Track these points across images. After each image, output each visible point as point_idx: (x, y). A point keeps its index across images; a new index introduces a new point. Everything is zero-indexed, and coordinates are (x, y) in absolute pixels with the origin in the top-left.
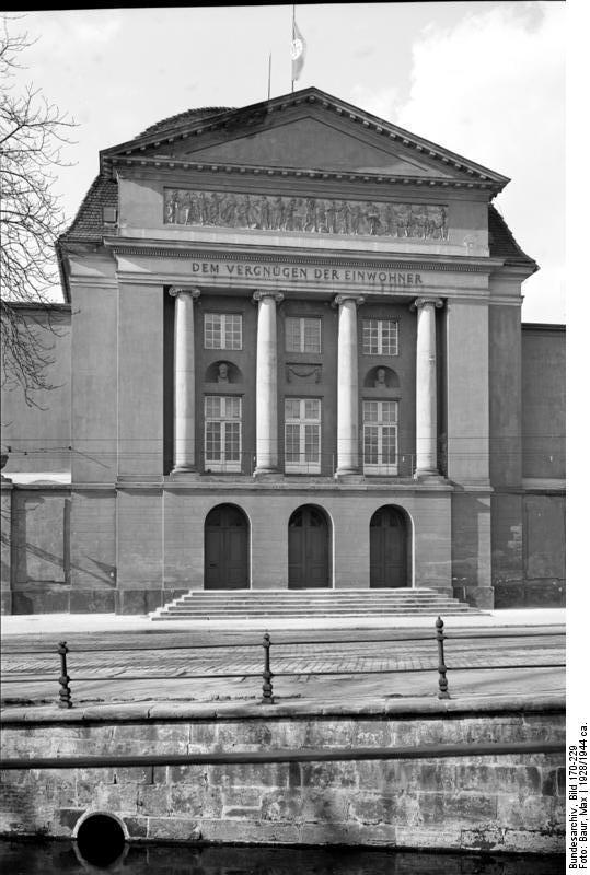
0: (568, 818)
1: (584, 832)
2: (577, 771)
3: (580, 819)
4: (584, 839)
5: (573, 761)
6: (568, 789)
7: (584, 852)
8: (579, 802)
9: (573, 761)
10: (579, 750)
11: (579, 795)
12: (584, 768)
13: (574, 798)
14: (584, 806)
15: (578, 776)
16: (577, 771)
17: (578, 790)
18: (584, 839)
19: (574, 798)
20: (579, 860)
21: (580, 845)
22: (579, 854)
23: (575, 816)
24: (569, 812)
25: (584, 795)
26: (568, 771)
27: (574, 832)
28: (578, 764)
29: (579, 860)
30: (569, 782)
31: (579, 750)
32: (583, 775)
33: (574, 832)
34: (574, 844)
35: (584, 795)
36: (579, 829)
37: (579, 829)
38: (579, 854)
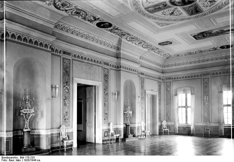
0: (15, 156)
1: (11, 160)
2: (28, 159)
3: (15, 159)
4: (10, 160)
5: (31, 157)
6: (23, 156)
7: (6, 161)
8: (20, 159)
9: (31, 157)
10: (33, 159)
11: (21, 159)
12: (29, 160)
13: (21, 158)
14: (18, 160)
15: (26, 159)
16: (28, 159)
17: (23, 159)
18: (10, 160)
19: (21, 158)
20: (4, 159)
22: (6, 159)
23: (16, 158)
24: (17, 156)
25: (21, 160)
26: (28, 156)
27: (11, 158)
28: (30, 159)
29: (4, 159)
30: (25, 156)
31: (33, 159)
33: (11, 158)
34: (8, 158)
35: (21, 160)
36: (12, 159)
37: (12, 159)
38: (6, 159)
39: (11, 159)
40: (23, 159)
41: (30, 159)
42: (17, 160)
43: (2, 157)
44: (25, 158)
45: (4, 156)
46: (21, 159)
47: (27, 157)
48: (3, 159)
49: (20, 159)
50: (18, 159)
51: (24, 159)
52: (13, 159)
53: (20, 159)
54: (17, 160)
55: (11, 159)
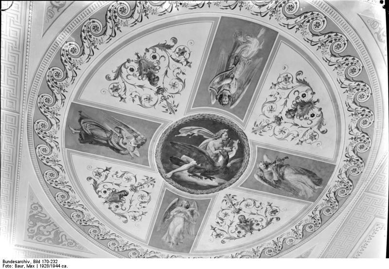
1: (19, 267)
2: (46, 263)
3: (25, 265)
4: (16, 266)
5: (51, 261)
7: (10, 267)
8: (32, 264)
9: (51, 261)
10: (56, 264)
11: (35, 264)
12: (48, 266)
13: (34, 262)
14: (31, 266)
15: (44, 264)
16: (46, 263)
17: (38, 264)
18: (16, 266)
19: (34, 262)
20: (7, 264)
22: (9, 264)
23: (26, 262)
25: (36, 266)
28: (49, 264)
29: (7, 264)
30: (41, 260)
31: (56, 264)
33: (19, 262)
35: (36, 266)
36: (21, 264)
37: (21, 264)
38: (9, 264)
39: (18, 264)
40: (39, 264)
41: (49, 264)
42: (28, 265)
44: (41, 263)
46: (35, 264)
47: (44, 261)
48: (5, 263)
49: (34, 264)
50: (30, 263)
51: (40, 264)
52: (22, 264)
53: (34, 264)
54: (28, 265)
55: (18, 264)
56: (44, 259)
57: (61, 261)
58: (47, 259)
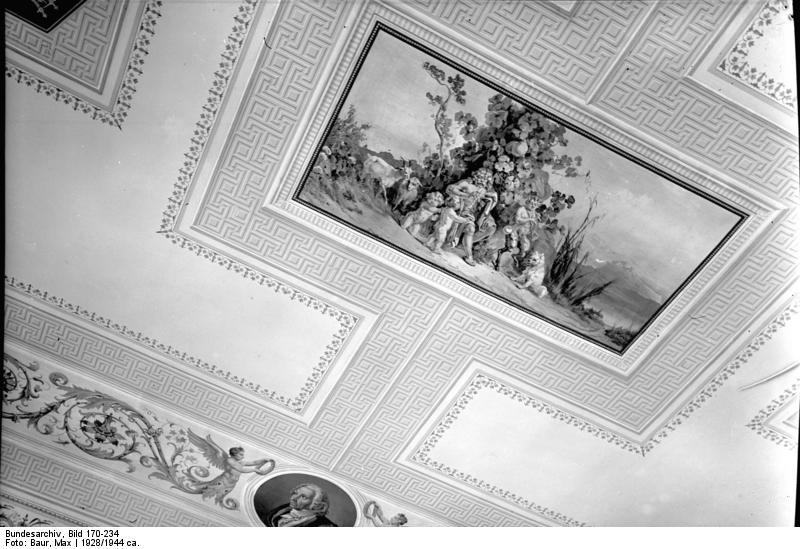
0: (52, 529)
2: (95, 538)
3: (51, 540)
4: (33, 543)
5: (105, 534)
6: (79, 529)
8: (67, 539)
9: (105, 534)
10: (115, 538)
11: (73, 540)
12: (98, 543)
13: (71, 534)
14: (63, 543)
15: (90, 538)
16: (95, 538)
17: (78, 538)
18: (33, 543)
19: (71, 534)
20: (14, 539)
21: (27, 540)
22: (19, 539)
23: (54, 535)
24: (58, 529)
25: (73, 543)
26: (95, 528)
27: (39, 535)
28: (101, 538)
29: (14, 539)
30: (85, 530)
32: (91, 543)
33: (39, 535)
34: (28, 534)
35: (73, 543)
36: (42, 539)
37: (42, 539)
38: (19, 539)
39: (37, 539)
40: (80, 540)
41: (101, 538)
42: (59, 541)
43: (8, 533)
44: (85, 536)
45: (13, 530)
47: (91, 533)
48: (10, 538)
51: (81, 539)
52: (46, 539)
54: (59, 541)
55: (37, 539)
56: (90, 529)
57: (126, 533)
58: (95, 528)
